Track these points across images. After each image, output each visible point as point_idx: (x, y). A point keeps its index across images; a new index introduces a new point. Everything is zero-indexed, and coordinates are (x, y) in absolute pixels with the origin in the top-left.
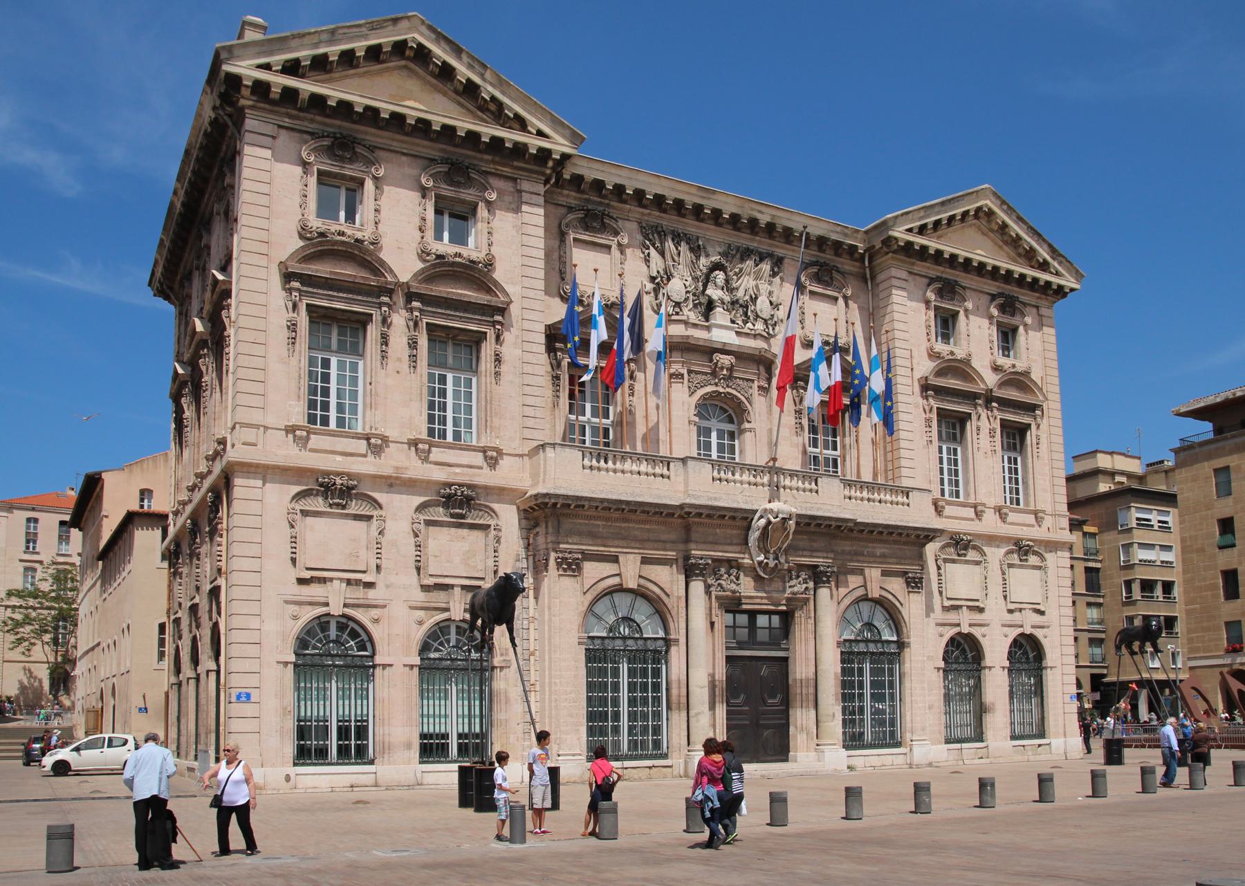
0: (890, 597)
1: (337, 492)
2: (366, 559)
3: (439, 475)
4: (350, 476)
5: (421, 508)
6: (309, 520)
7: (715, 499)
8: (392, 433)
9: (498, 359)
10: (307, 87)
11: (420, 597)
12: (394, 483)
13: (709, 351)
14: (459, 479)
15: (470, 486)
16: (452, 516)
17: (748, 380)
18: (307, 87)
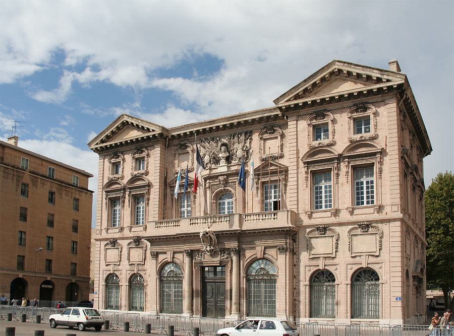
0: (270, 257)
1: (114, 243)
2: (117, 259)
3: (131, 235)
4: (114, 239)
5: (128, 244)
6: (108, 250)
7: (189, 230)
8: (124, 226)
9: (148, 200)
10: (108, 144)
11: (128, 267)
12: (123, 239)
13: (216, 177)
14: (136, 235)
15: (138, 237)
16: (136, 245)
17: (234, 182)
18: (108, 144)
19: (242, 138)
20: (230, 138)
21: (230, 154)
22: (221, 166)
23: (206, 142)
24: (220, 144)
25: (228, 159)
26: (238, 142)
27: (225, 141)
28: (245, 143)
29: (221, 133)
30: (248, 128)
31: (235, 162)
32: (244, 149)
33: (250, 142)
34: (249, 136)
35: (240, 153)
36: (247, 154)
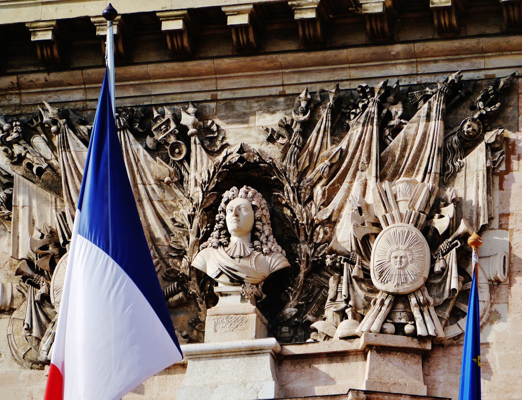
19: (424, 128)
20: (307, 127)
21: (291, 256)
22: (218, 354)
23: (73, 140)
24: (201, 167)
25: (286, 305)
26: (381, 163)
27: (249, 135)
28: (446, 176)
29: (218, 72)
30: (482, 53)
31: (345, 327)
32: (441, 224)
33: (496, 176)
34: (487, 122)
35: (396, 258)
36: (462, 271)
